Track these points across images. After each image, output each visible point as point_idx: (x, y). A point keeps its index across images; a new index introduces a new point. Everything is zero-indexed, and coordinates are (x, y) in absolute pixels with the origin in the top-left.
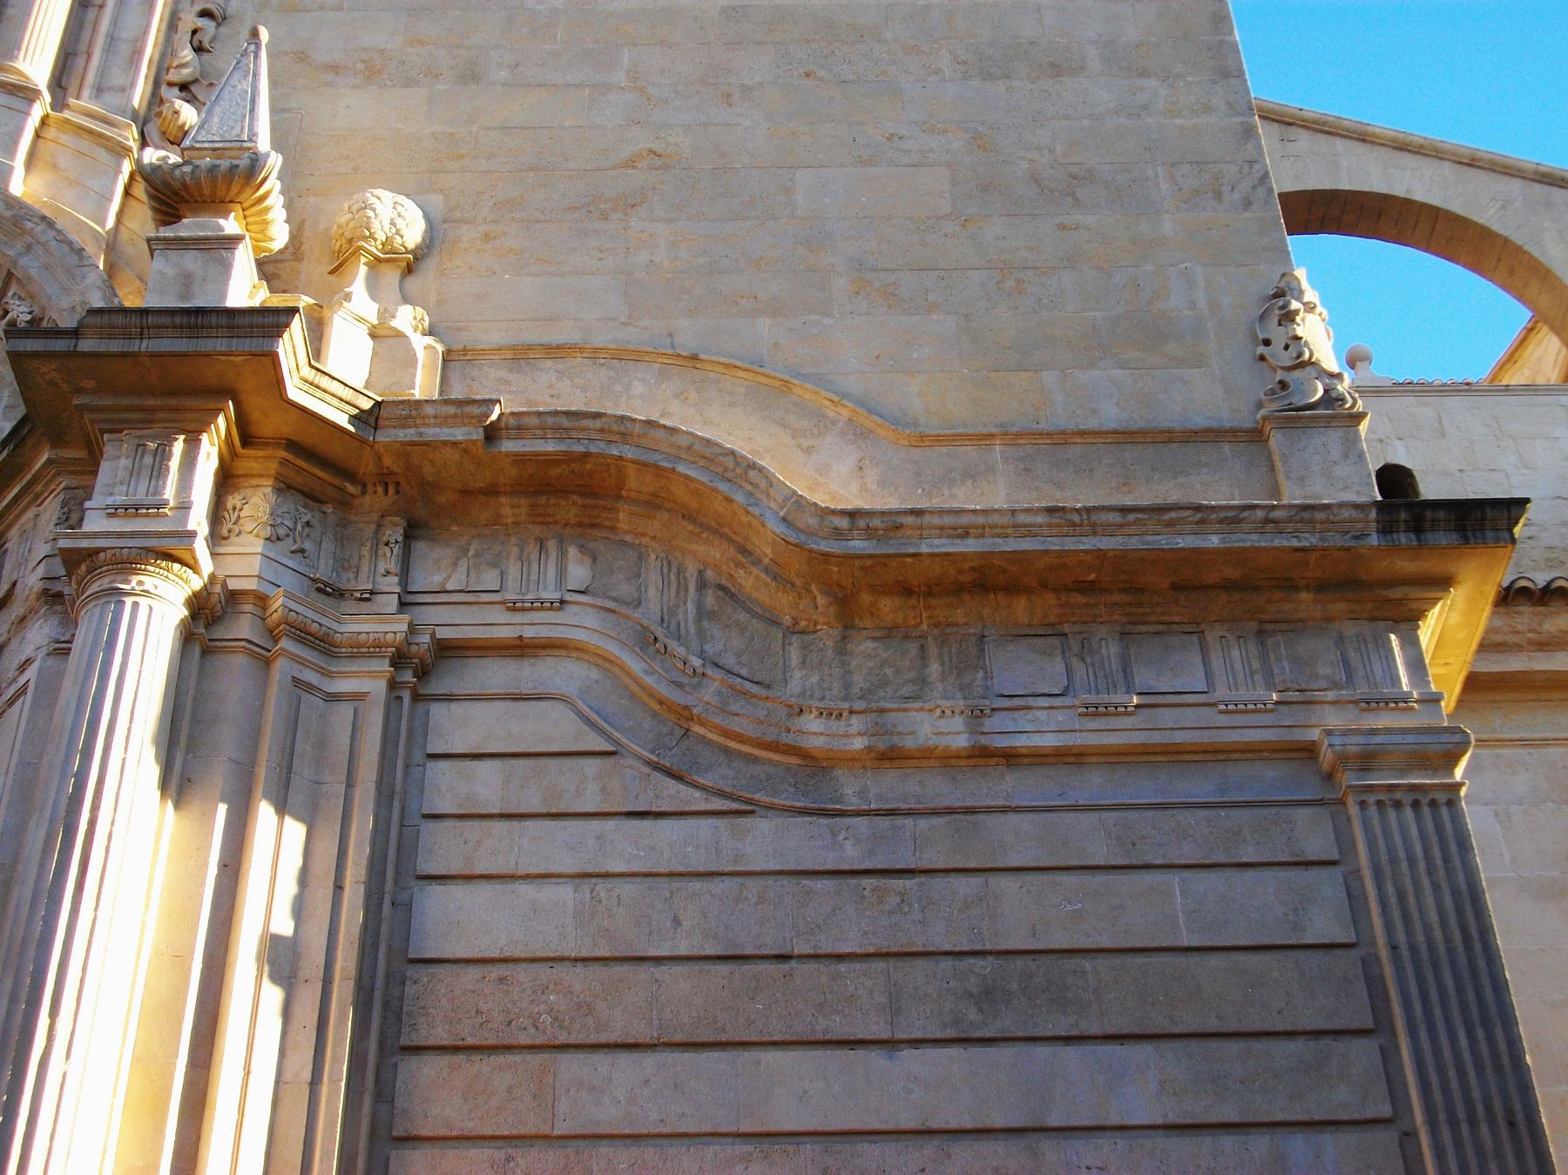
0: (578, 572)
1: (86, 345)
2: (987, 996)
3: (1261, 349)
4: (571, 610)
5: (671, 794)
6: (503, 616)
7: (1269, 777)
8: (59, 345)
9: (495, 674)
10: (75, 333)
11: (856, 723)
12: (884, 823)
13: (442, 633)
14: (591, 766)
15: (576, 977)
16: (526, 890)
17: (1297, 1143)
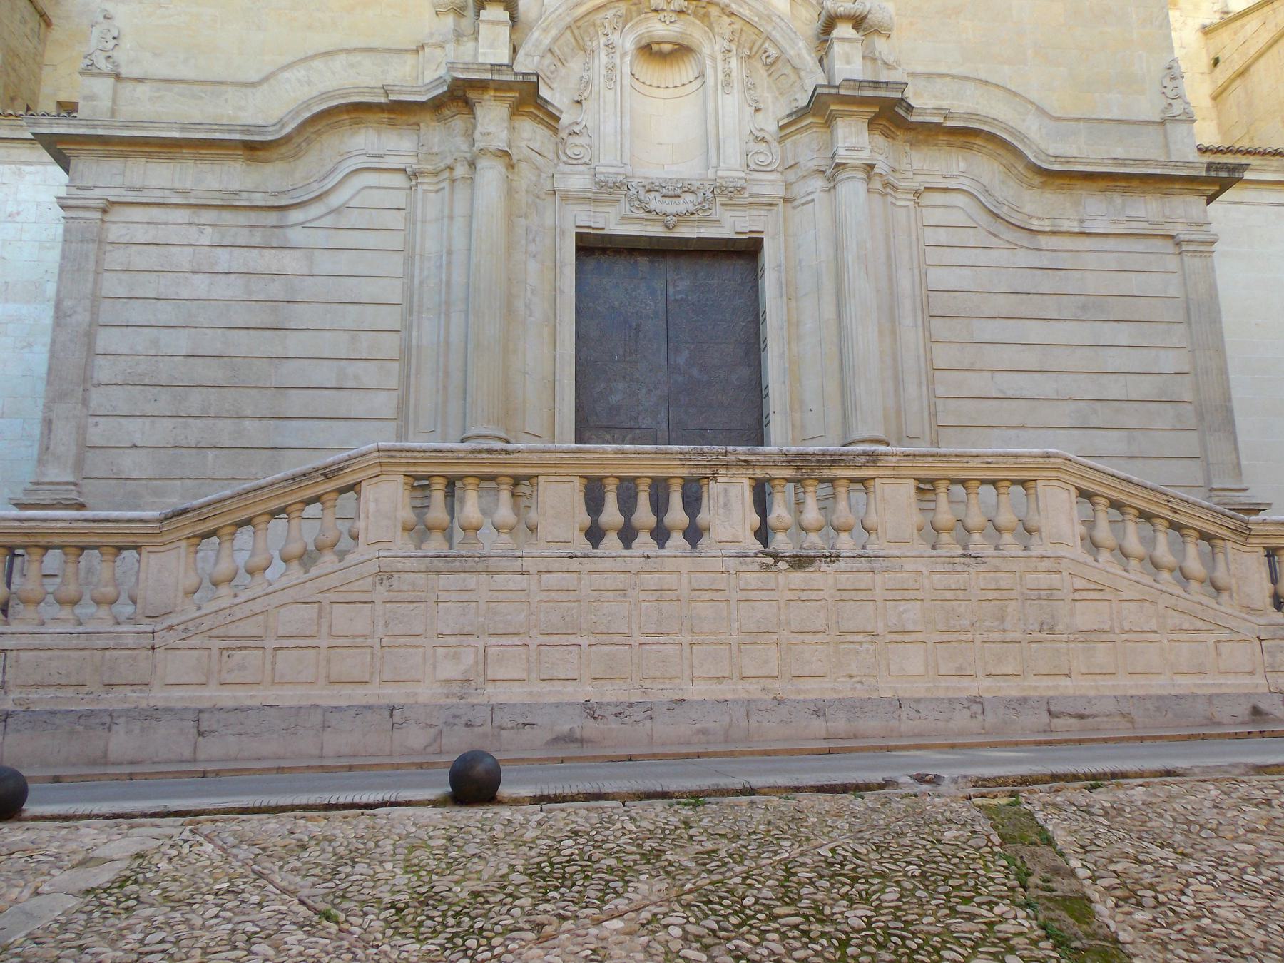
0: (962, 165)
1: (842, 92)
2: (1084, 308)
3: (1164, 90)
4: (961, 179)
5: (995, 242)
6: (942, 180)
7: (1159, 243)
8: (833, 91)
9: (938, 198)
10: (838, 87)
11: (1047, 222)
12: (1054, 254)
13: (927, 185)
14: (971, 231)
15: (975, 297)
16: (958, 270)
17: (1162, 352)
